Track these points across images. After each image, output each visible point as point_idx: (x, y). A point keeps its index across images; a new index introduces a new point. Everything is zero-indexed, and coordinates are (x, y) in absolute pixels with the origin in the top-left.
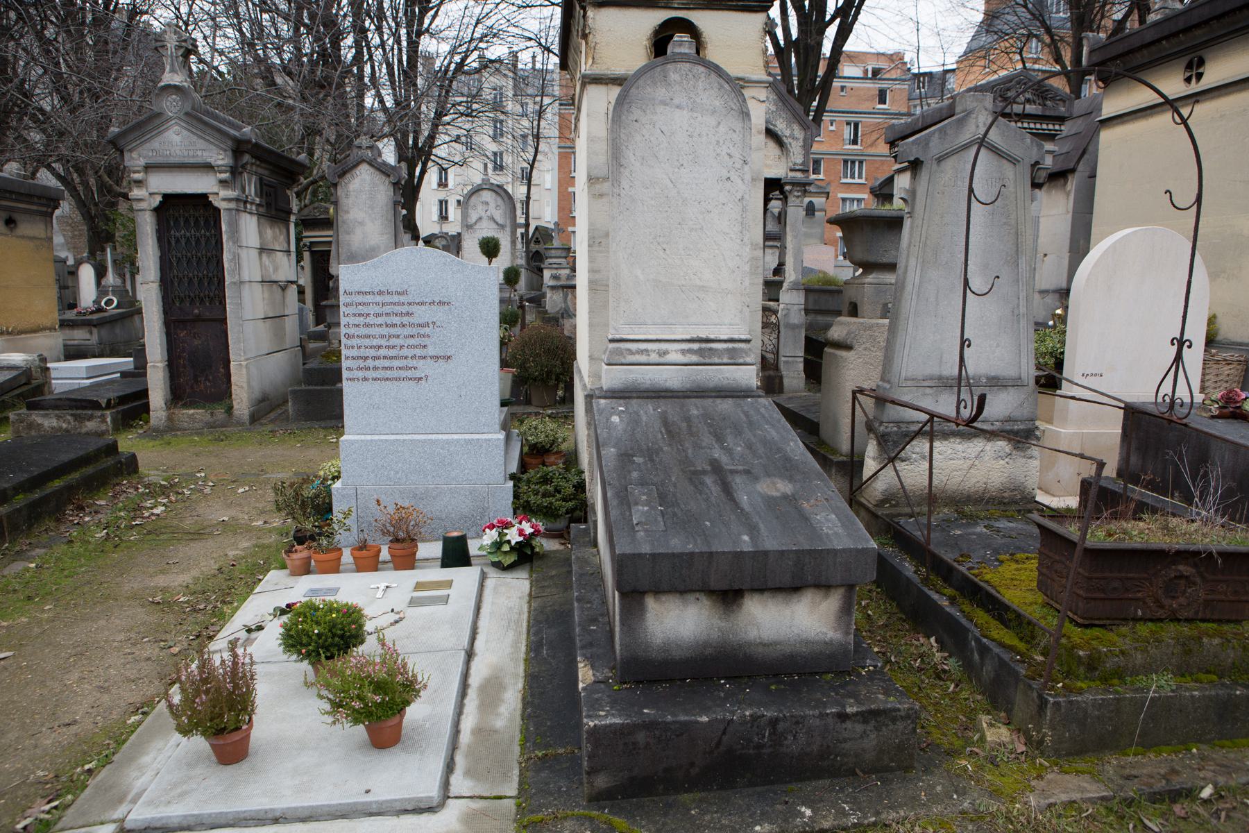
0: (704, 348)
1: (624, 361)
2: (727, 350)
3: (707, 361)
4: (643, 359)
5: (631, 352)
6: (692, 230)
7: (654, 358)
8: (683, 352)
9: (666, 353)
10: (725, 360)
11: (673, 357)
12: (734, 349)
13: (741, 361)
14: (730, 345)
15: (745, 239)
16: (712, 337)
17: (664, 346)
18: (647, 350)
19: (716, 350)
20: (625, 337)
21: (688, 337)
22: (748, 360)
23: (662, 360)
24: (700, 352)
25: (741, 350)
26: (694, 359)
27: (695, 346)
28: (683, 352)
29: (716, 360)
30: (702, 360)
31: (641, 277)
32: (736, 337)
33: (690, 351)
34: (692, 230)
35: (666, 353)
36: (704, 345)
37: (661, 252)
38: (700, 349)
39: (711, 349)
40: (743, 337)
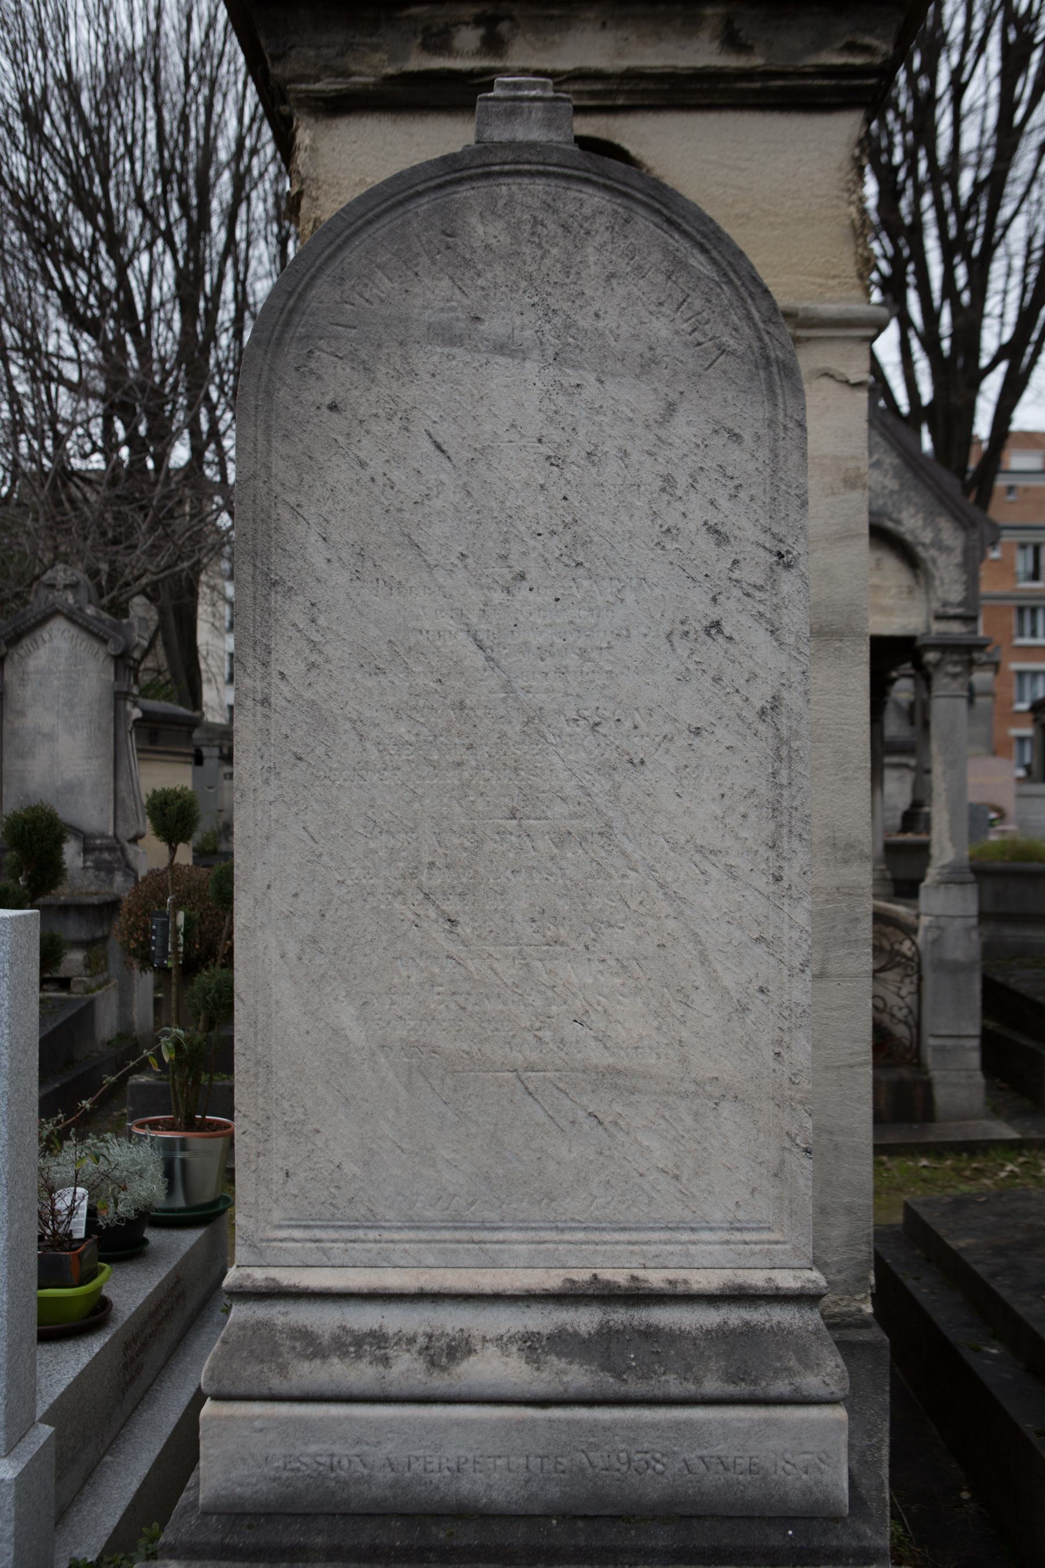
0: (619, 1334)
1: (277, 1384)
2: (722, 1335)
3: (635, 1387)
4: (361, 1374)
5: (310, 1344)
6: (562, 838)
7: (406, 1369)
8: (532, 1346)
9: (458, 1348)
10: (712, 1386)
11: (492, 1368)
12: (749, 1332)
13: (781, 1387)
14: (735, 1316)
15: (791, 873)
16: (656, 1279)
17: (452, 1320)
18: (378, 1338)
19: (673, 1337)
20: (287, 1278)
21: (553, 1280)
22: (812, 1383)
23: (439, 1383)
24: (602, 1347)
25: (780, 1335)
26: (578, 1377)
27: (585, 1320)
28: (532, 1346)
29: (674, 1386)
30: (610, 1384)
31: (357, 1034)
32: (757, 1279)
33: (562, 1342)
34: (562, 838)
35: (458, 1348)
36: (620, 1316)
37: (438, 932)
38: (607, 1334)
39: (650, 1334)
40: (787, 1280)
